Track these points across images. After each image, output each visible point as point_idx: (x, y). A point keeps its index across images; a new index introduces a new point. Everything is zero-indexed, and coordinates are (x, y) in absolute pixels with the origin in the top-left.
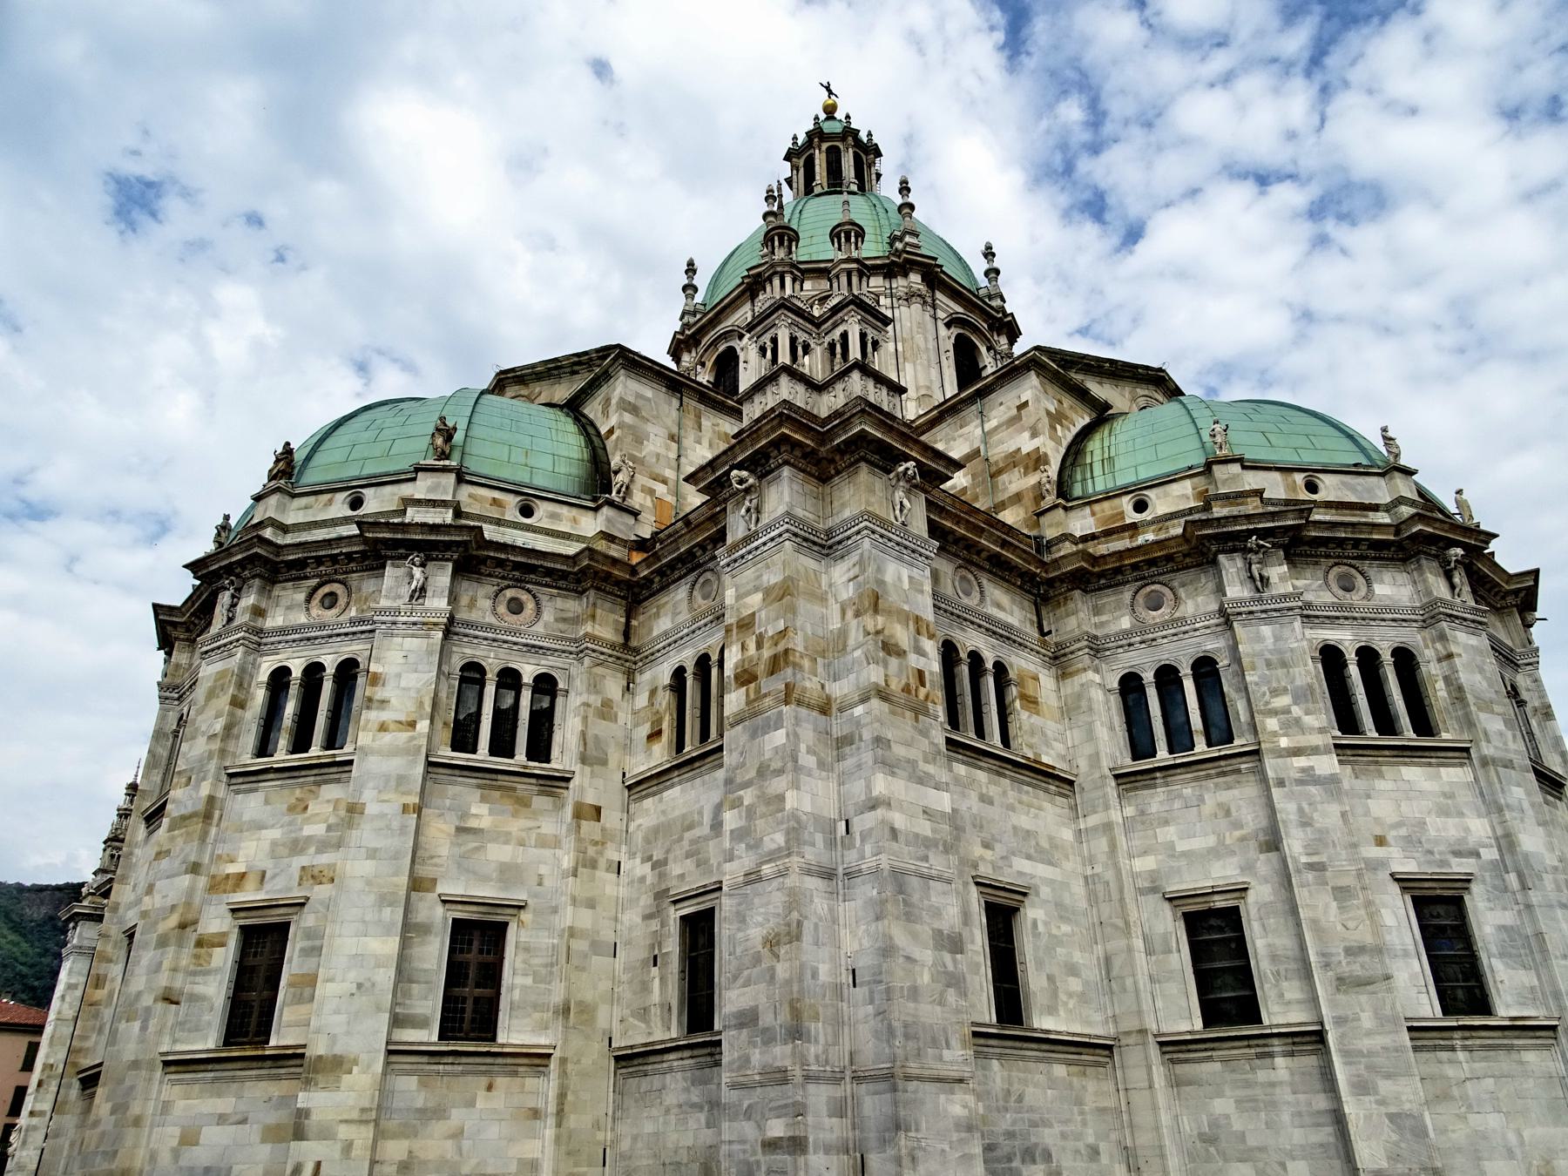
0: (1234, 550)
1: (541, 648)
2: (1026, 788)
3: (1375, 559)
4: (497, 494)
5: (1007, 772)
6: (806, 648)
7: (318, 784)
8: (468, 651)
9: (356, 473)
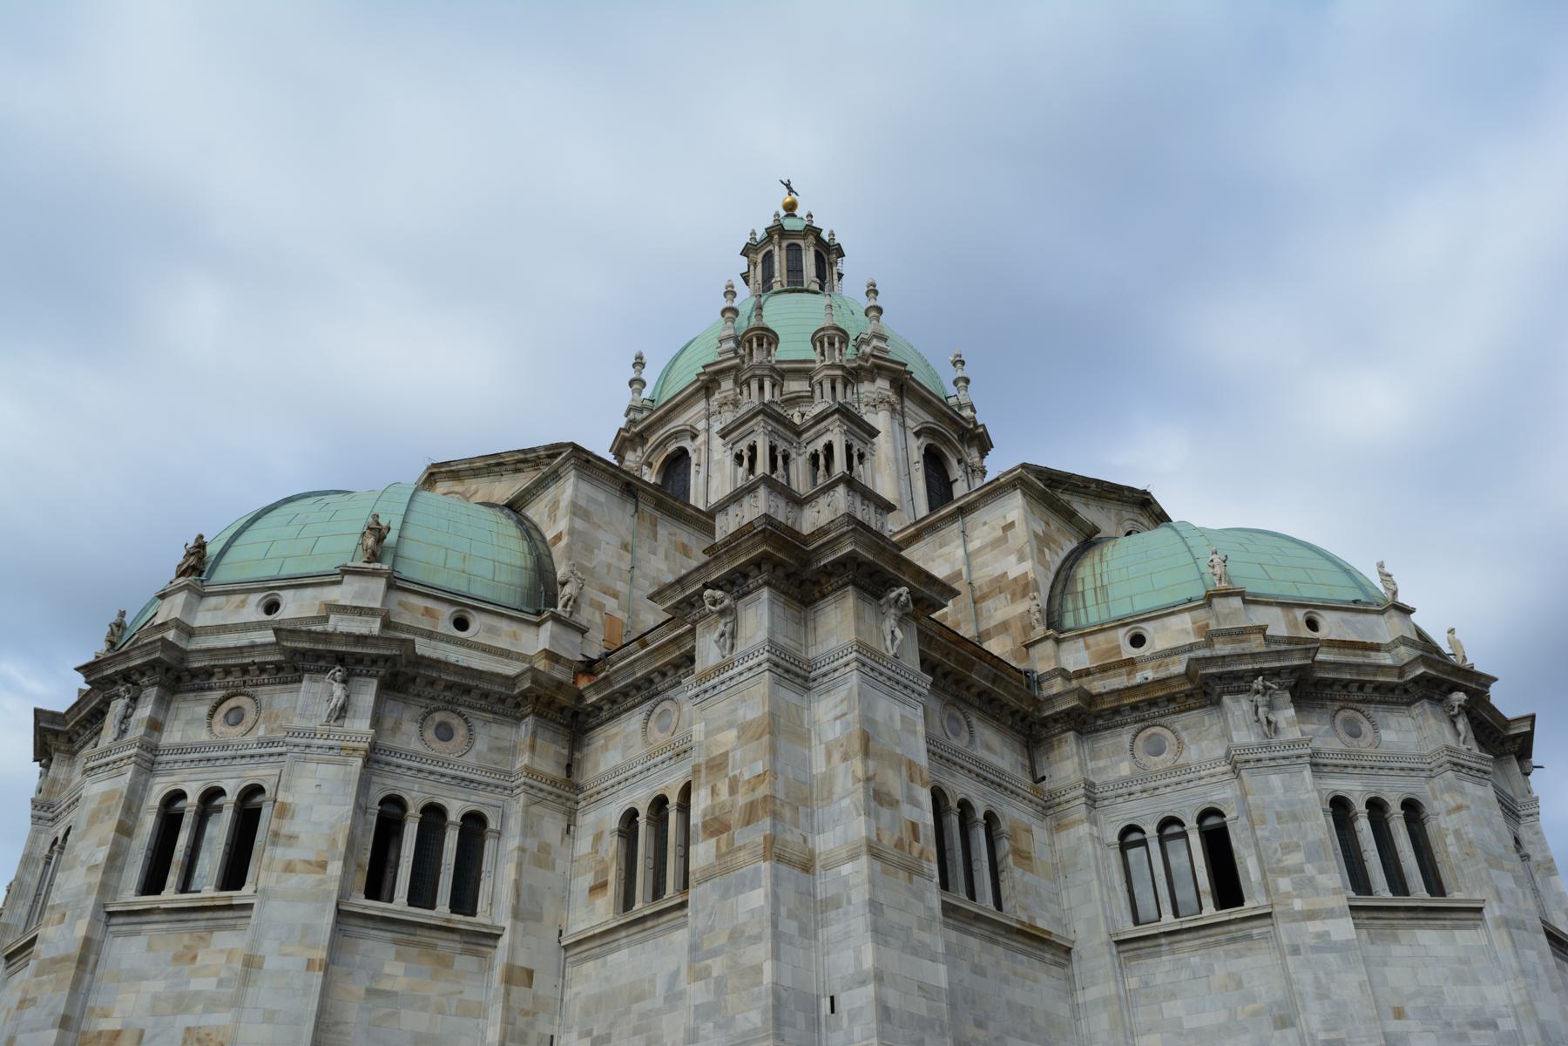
0: (1240, 692)
1: (472, 781)
2: (1020, 957)
3: (1380, 702)
4: (430, 604)
5: (1000, 939)
6: (787, 795)
7: (210, 930)
9: (275, 573)
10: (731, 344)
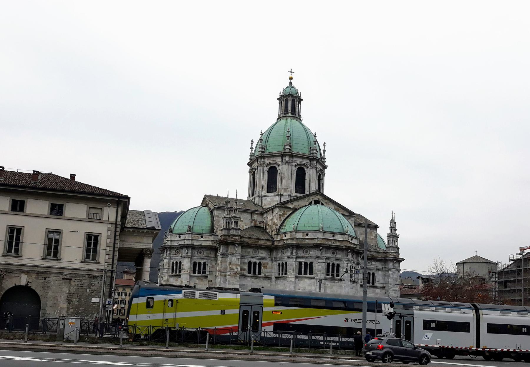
8: (194, 260)
10: (260, 150)
